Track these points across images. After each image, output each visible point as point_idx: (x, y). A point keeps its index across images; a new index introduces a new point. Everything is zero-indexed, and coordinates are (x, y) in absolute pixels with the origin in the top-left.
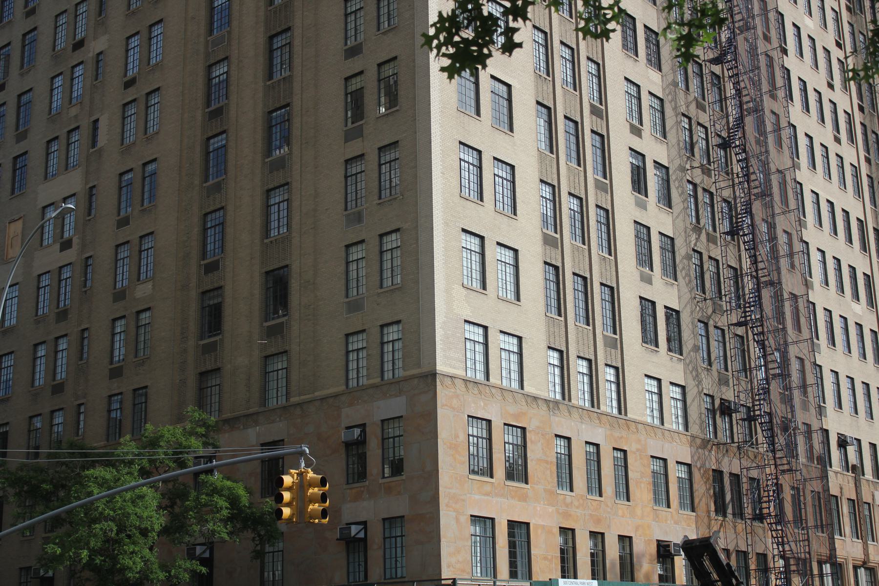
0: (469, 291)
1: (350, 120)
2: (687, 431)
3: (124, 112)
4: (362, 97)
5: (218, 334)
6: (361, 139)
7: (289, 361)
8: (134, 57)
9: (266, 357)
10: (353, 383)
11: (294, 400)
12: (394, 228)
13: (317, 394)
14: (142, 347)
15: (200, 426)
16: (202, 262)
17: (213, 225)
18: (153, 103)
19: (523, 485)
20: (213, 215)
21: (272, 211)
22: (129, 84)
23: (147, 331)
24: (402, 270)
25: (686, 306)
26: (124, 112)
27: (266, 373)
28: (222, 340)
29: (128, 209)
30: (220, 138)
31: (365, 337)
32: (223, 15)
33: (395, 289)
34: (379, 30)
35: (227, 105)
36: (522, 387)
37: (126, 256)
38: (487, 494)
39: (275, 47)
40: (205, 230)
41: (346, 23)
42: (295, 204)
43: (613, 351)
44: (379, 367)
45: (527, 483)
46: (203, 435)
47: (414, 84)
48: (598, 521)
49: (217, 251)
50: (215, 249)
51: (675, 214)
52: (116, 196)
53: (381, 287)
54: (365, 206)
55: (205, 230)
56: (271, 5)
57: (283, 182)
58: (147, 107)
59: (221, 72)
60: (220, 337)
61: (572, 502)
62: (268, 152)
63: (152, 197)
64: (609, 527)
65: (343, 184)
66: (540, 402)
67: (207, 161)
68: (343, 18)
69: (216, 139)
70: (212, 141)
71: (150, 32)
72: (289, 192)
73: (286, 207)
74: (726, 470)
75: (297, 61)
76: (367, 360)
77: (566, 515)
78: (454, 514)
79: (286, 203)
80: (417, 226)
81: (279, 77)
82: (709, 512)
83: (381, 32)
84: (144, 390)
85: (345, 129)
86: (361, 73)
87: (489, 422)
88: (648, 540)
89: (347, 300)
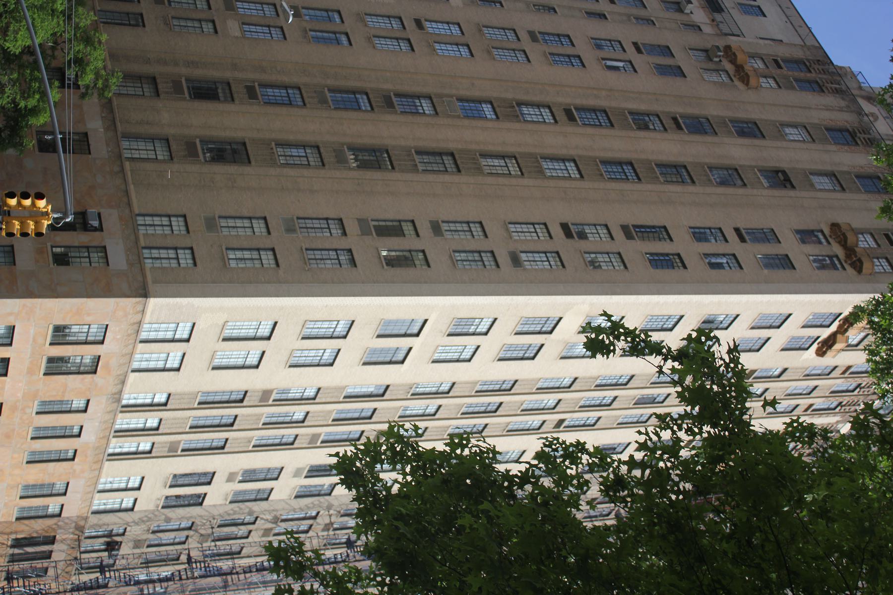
0: (221, 327)
1: (376, 223)
2: (93, 513)
3: (394, 17)
4: (397, 235)
5: (190, 97)
6: (360, 233)
7: (164, 161)
8: (442, 29)
9: (167, 140)
10: (140, 220)
11: (127, 165)
12: (280, 261)
13: (132, 187)
14: (182, 24)
15: (103, 84)
16: (256, 84)
17: (290, 95)
18: (401, 44)
19: (42, 372)
20: (299, 96)
21: (299, 151)
22: (419, 24)
23: (197, 29)
24: (242, 268)
25: (207, 511)
26: (394, 17)
27: (153, 139)
28: (185, 99)
29: (307, 17)
30: (368, 105)
31: (182, 232)
32: (474, 112)
33: (224, 261)
34: (454, 251)
35: (396, 113)
36: (133, 371)
37: (266, 12)
38: (34, 340)
39: (444, 158)
40: (286, 88)
41: (461, 222)
42: (305, 172)
43: (167, 449)
44: (155, 245)
45: (45, 374)
46: (95, 85)
47: (405, 283)
49: (267, 97)
50: (268, 96)
51: (289, 502)
52: (319, 6)
53: (227, 249)
54: (300, 236)
55: (286, 88)
56: (480, 155)
57: (325, 161)
58: (397, 39)
59: (425, 108)
60: (188, 98)
61: (26, 413)
62: (353, 149)
63: (317, 39)
65: (321, 216)
66: (119, 387)
67: (347, 92)
68: (466, 220)
69: (366, 101)
70: (365, 97)
71: (462, 45)
72: (316, 167)
73: (303, 163)
74: (55, 547)
75: (431, 177)
76: (162, 234)
77: (14, 409)
79: (306, 163)
80: (280, 282)
81: (417, 161)
82: (16, 533)
83: (452, 254)
84: (141, 24)
85: (369, 219)
86: (418, 235)
87: (102, 342)
89: (217, 218)
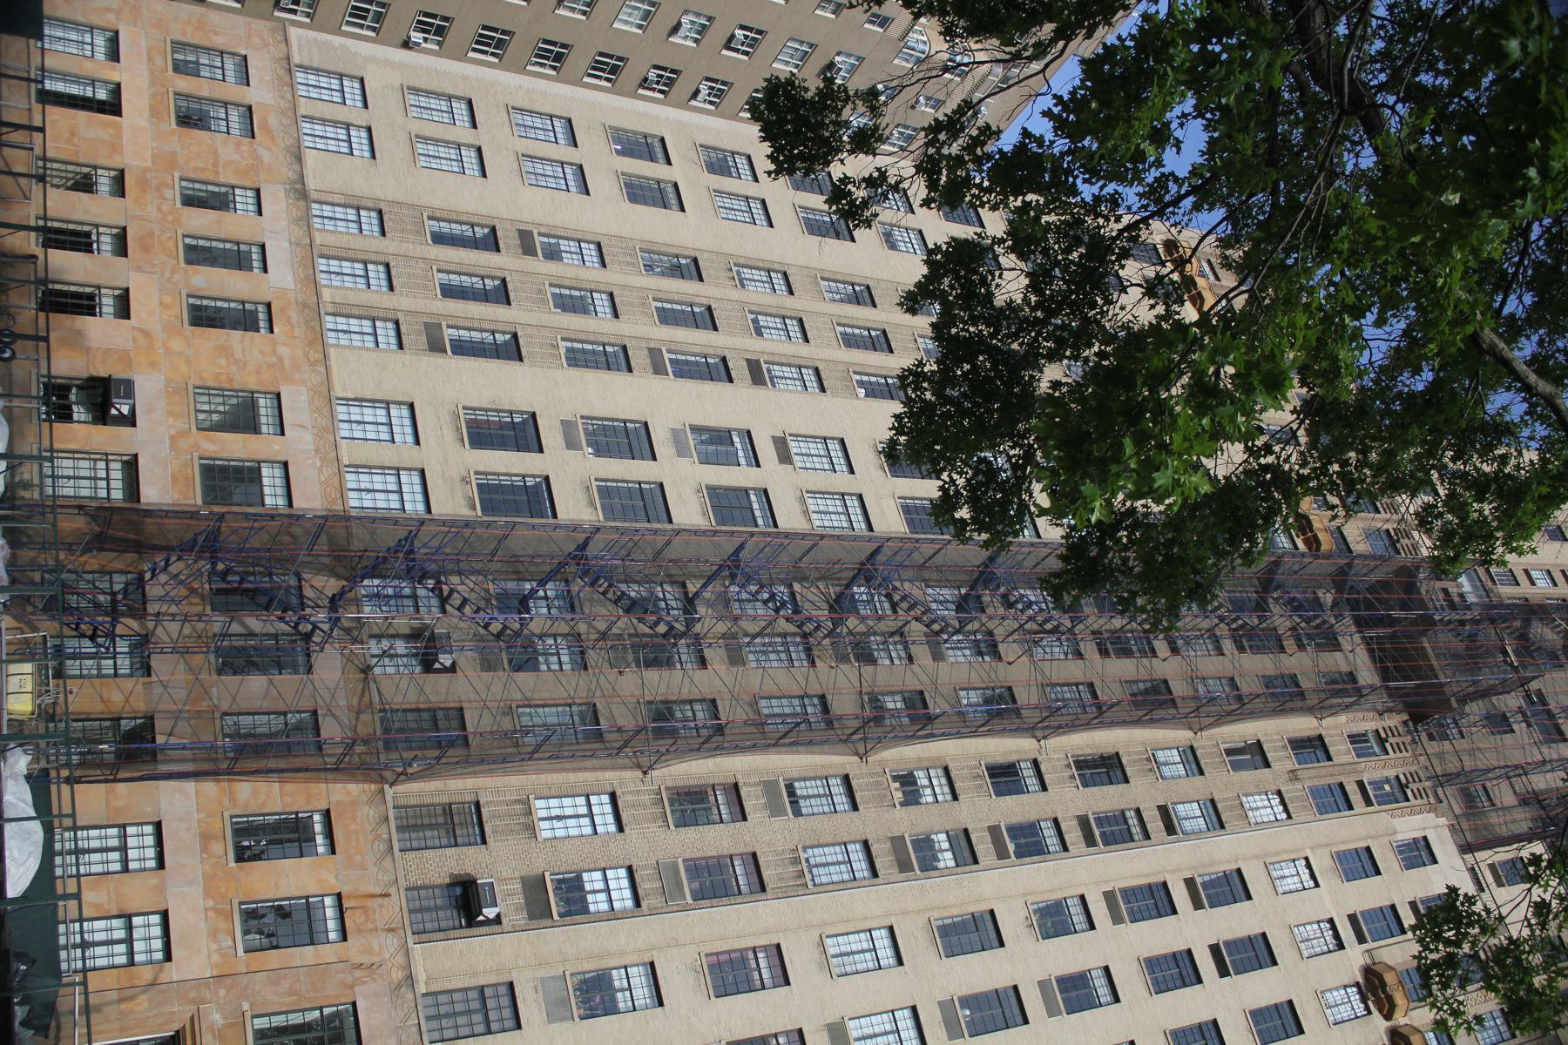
38: (150, 59)
48: (146, 248)
61: (165, 199)
64: (139, 269)
77: (144, 184)
88: (130, 359)
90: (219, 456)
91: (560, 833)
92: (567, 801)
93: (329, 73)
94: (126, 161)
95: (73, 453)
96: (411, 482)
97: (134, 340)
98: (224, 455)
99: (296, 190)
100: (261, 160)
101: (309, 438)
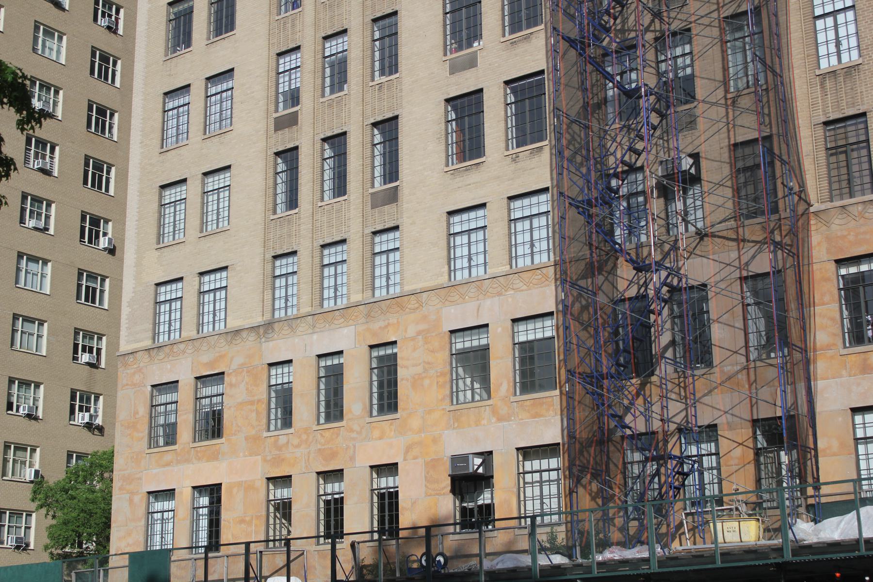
38: (168, 464)
48: (334, 455)
61: (288, 442)
64: (352, 459)
77: (278, 461)
78: (127, 496)
90: (512, 379)
91: (853, 42)
92: (821, 38)
93: (156, 314)
94: (259, 477)
95: (521, 501)
96: (521, 208)
97: (415, 458)
98: (511, 374)
99: (265, 332)
100: (242, 364)
101: (488, 302)
